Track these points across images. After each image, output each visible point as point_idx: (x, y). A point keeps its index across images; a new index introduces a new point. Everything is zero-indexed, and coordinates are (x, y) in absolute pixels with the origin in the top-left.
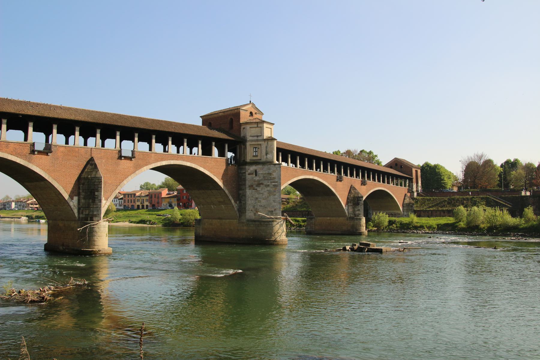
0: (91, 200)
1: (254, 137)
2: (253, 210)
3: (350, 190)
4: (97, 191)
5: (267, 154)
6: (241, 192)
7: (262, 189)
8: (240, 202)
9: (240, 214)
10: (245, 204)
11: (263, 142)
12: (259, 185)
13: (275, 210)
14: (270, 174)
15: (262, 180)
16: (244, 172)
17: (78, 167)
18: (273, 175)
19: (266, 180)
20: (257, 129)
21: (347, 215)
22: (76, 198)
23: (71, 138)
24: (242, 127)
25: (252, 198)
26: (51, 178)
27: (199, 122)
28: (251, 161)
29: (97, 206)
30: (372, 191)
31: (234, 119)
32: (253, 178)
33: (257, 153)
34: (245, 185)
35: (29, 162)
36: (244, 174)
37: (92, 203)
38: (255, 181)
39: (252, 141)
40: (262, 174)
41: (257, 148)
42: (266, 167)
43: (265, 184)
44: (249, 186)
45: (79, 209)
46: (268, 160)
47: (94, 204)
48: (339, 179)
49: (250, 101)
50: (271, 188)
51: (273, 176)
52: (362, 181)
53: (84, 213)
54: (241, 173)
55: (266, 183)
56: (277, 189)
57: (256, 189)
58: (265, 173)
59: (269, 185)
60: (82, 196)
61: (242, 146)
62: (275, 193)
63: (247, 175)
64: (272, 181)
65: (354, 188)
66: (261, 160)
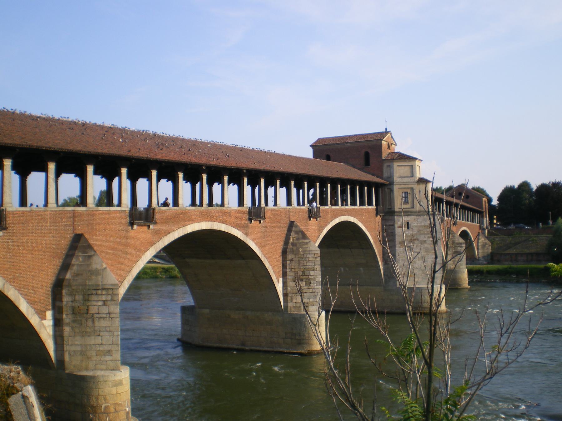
0: (304, 283)
1: (403, 178)
4: (313, 270)
15: (415, 234)
16: (392, 224)
19: (422, 234)
24: (385, 165)
25: (404, 258)
27: (309, 154)
29: (314, 291)
33: (406, 198)
35: (247, 235)
36: (391, 227)
37: (305, 286)
40: (416, 226)
41: (406, 193)
43: (421, 239)
44: (400, 243)
45: (285, 295)
47: (309, 287)
50: (429, 244)
53: (294, 301)
58: (421, 226)
59: (426, 241)
61: (386, 190)
66: (413, 208)
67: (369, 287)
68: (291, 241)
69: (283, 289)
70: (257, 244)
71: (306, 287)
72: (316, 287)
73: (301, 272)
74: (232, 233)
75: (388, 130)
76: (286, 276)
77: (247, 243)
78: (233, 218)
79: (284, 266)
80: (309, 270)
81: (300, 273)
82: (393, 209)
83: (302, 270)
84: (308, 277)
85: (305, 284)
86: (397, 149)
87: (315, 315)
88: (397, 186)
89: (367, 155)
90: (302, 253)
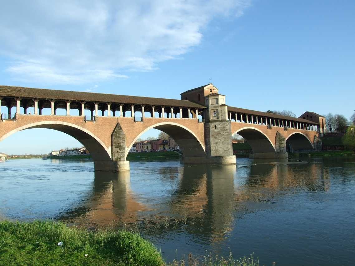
1: (214, 105)
3: (276, 134)
6: (207, 139)
10: (210, 146)
12: (218, 134)
13: (229, 149)
15: (219, 131)
16: (208, 127)
17: (111, 129)
21: (275, 150)
22: (110, 148)
23: (106, 112)
24: (206, 99)
26: (95, 136)
27: (179, 98)
30: (291, 134)
34: (209, 135)
35: (83, 127)
36: (208, 128)
42: (222, 123)
44: (212, 136)
45: (112, 154)
46: (223, 119)
48: (269, 127)
50: (226, 136)
52: (284, 129)
53: (115, 156)
55: (222, 133)
57: (216, 137)
63: (210, 129)
64: (226, 132)
65: (279, 133)
66: (218, 118)
68: (115, 131)
70: (90, 131)
74: (72, 126)
79: (112, 141)
81: (117, 144)
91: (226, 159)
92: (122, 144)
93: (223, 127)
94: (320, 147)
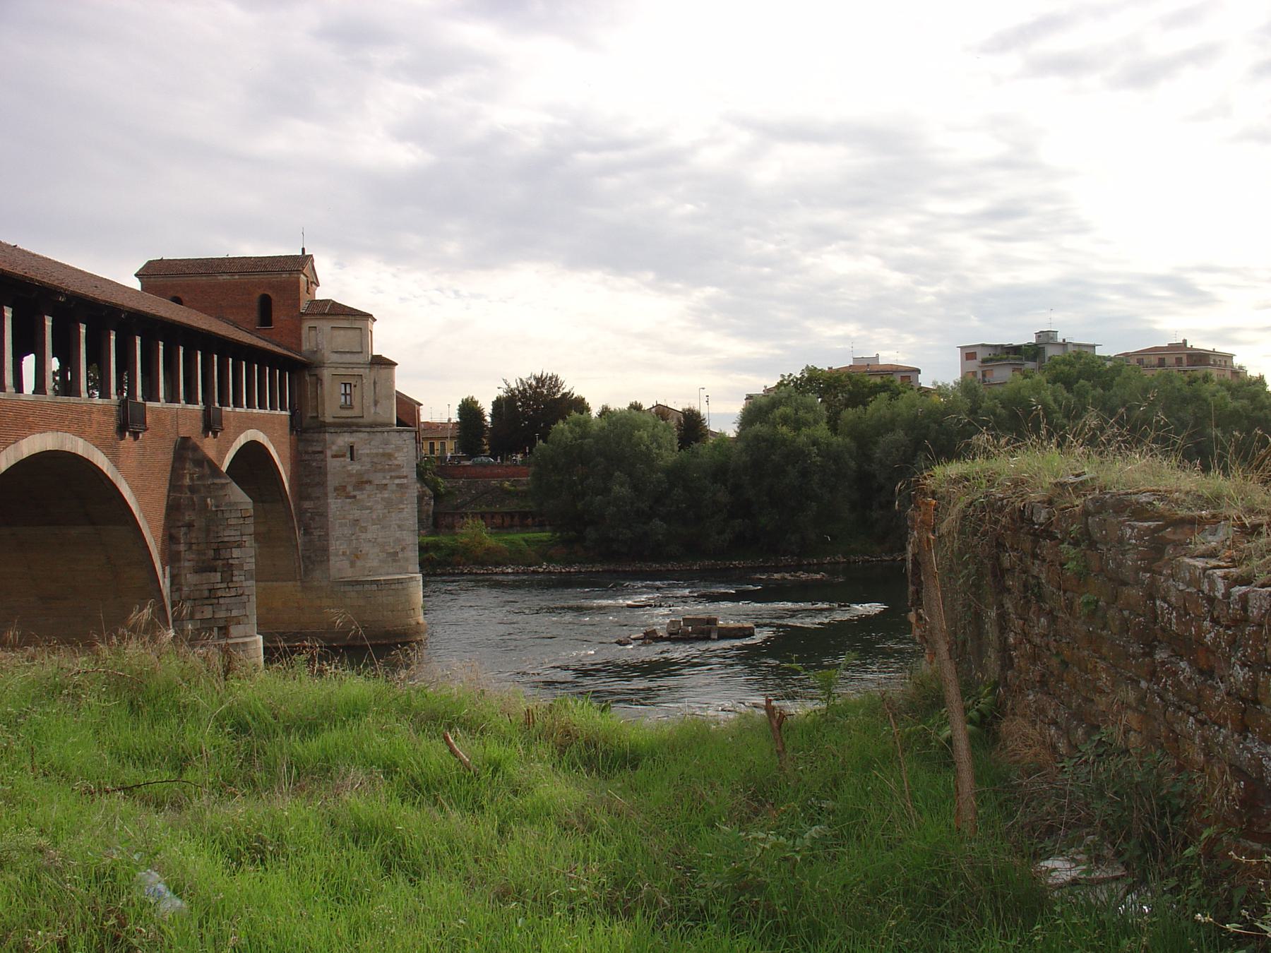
0: (219, 574)
1: (344, 356)
2: (348, 553)
4: (239, 547)
5: (376, 403)
6: (307, 505)
7: (369, 496)
8: (307, 532)
9: (306, 567)
11: (368, 370)
12: (361, 484)
13: (403, 549)
14: (390, 456)
18: (396, 458)
20: (350, 333)
24: (307, 324)
28: (337, 420)
31: (273, 296)
32: (344, 467)
33: (348, 397)
34: (323, 484)
37: (222, 582)
38: (350, 475)
39: (337, 365)
44: (336, 489)
46: (380, 420)
49: (303, 250)
50: (393, 492)
51: (396, 462)
53: (198, 616)
54: (306, 453)
55: (378, 479)
56: (407, 495)
57: (354, 497)
58: (377, 454)
60: (187, 564)
61: (308, 378)
62: (402, 506)
63: (329, 459)
64: (393, 474)
67: (269, 583)
69: (171, 592)
71: (224, 585)
72: (245, 584)
73: (213, 551)
75: (306, 253)
76: (179, 560)
77: (118, 485)
78: (95, 426)
80: (228, 545)
82: (322, 419)
83: (215, 546)
84: (228, 564)
85: (220, 577)
86: (321, 294)
87: (256, 642)
88: (329, 369)
89: (266, 303)
90: (214, 509)
91: (403, 589)
92: (236, 553)
93: (383, 455)
94: (428, 516)
